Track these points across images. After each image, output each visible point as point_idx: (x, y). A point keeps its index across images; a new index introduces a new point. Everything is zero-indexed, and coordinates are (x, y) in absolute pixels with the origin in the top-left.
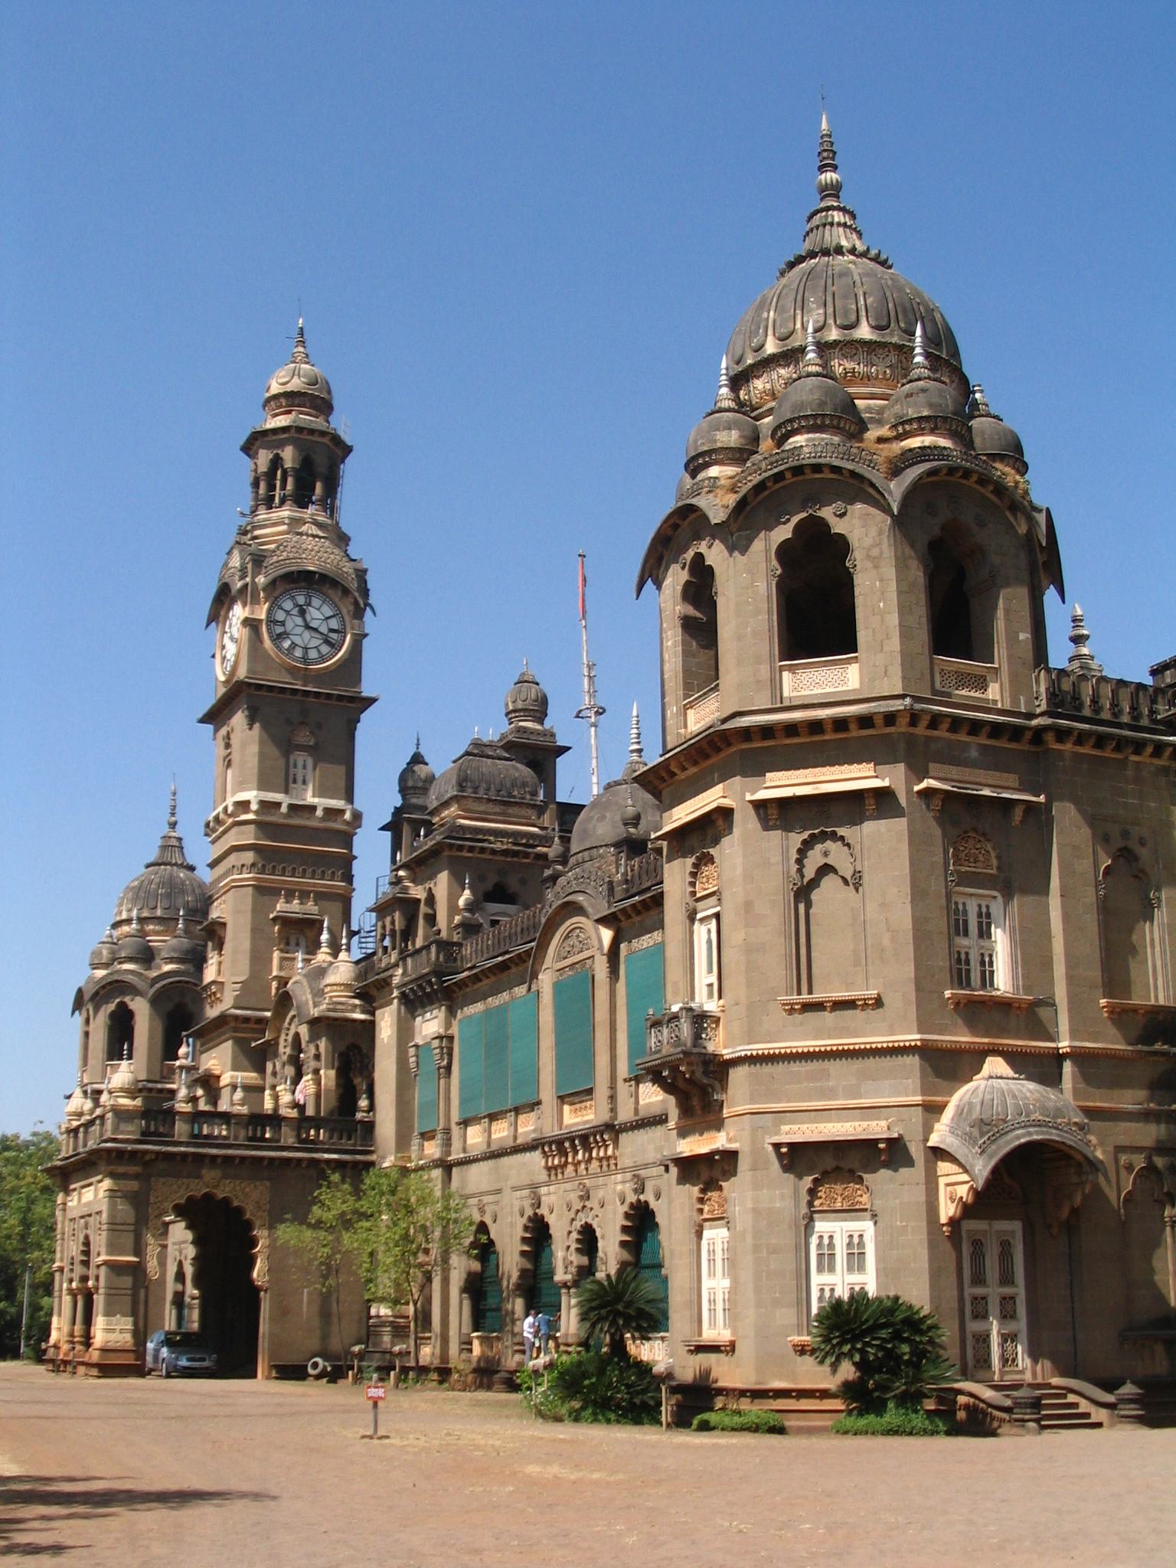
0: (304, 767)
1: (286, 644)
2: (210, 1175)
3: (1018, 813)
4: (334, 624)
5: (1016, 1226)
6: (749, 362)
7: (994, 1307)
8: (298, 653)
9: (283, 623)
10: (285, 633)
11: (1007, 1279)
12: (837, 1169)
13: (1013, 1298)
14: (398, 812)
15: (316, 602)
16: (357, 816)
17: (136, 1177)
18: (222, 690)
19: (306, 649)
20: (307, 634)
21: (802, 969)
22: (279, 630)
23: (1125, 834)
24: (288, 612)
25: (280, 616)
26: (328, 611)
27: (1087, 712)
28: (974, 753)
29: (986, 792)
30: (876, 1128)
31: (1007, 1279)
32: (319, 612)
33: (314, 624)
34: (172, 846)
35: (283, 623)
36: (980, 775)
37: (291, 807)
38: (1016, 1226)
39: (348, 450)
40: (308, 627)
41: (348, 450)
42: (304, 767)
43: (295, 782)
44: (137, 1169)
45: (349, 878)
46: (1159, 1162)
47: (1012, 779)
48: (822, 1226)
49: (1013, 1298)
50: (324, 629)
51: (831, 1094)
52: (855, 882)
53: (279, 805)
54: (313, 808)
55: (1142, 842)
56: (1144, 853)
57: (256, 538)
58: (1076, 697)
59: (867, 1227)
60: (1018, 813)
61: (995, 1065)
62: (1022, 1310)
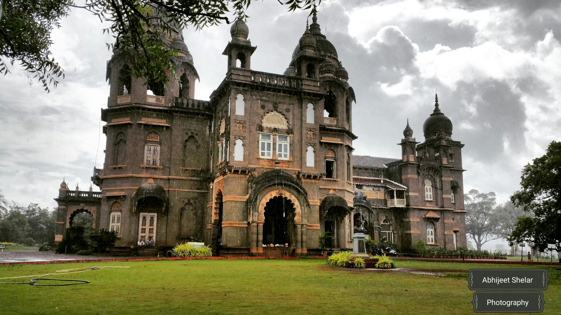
2: (82, 205)
3: (164, 129)
5: (156, 214)
7: (147, 231)
11: (151, 224)
12: (116, 202)
13: (153, 229)
17: (64, 205)
21: (115, 161)
23: (192, 133)
27: (185, 106)
28: (155, 115)
29: (154, 124)
30: (122, 193)
31: (151, 224)
36: (157, 120)
38: (156, 214)
44: (64, 203)
46: (192, 201)
47: (164, 121)
48: (112, 214)
49: (153, 229)
51: (116, 187)
52: (125, 142)
55: (197, 135)
56: (196, 137)
58: (182, 104)
59: (120, 213)
60: (164, 129)
61: (151, 181)
62: (155, 231)
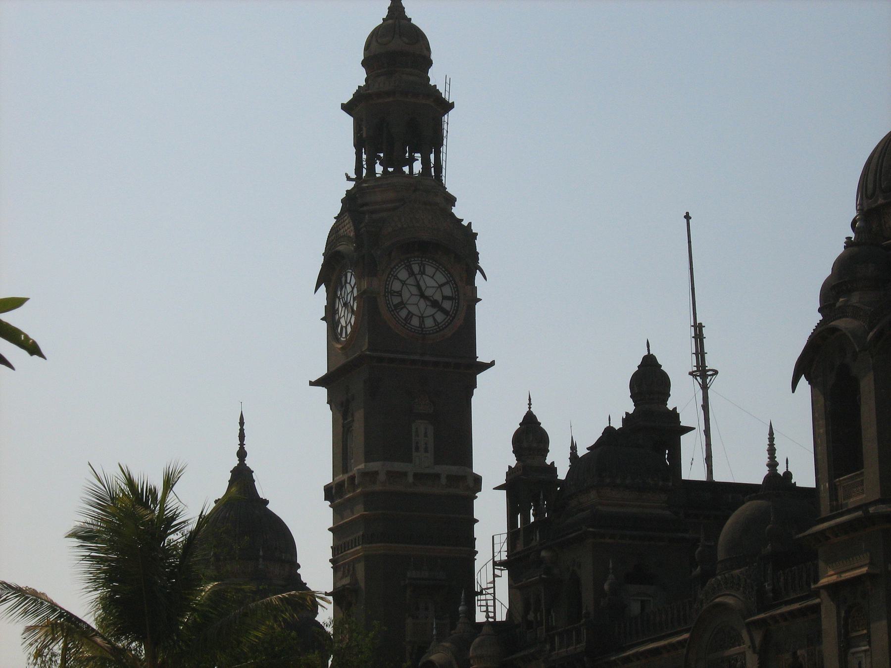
0: (426, 435)
1: (403, 313)
4: (448, 291)
6: (881, 201)
8: (415, 322)
9: (399, 294)
10: (402, 303)
14: (511, 472)
15: (429, 270)
16: (477, 482)
18: (342, 360)
19: (422, 318)
20: (422, 304)
22: (396, 300)
24: (404, 283)
25: (397, 286)
26: (441, 278)
32: (432, 281)
33: (429, 292)
34: (242, 476)
35: (399, 294)
37: (418, 476)
39: (448, 107)
40: (422, 295)
41: (448, 107)
42: (426, 435)
43: (417, 449)
45: (470, 541)
50: (438, 297)
53: (405, 474)
54: (437, 476)
57: (366, 204)
